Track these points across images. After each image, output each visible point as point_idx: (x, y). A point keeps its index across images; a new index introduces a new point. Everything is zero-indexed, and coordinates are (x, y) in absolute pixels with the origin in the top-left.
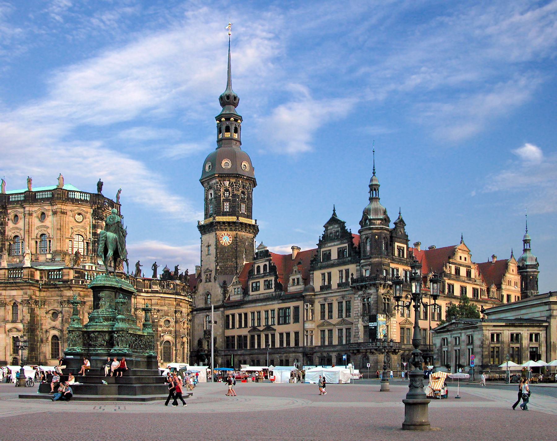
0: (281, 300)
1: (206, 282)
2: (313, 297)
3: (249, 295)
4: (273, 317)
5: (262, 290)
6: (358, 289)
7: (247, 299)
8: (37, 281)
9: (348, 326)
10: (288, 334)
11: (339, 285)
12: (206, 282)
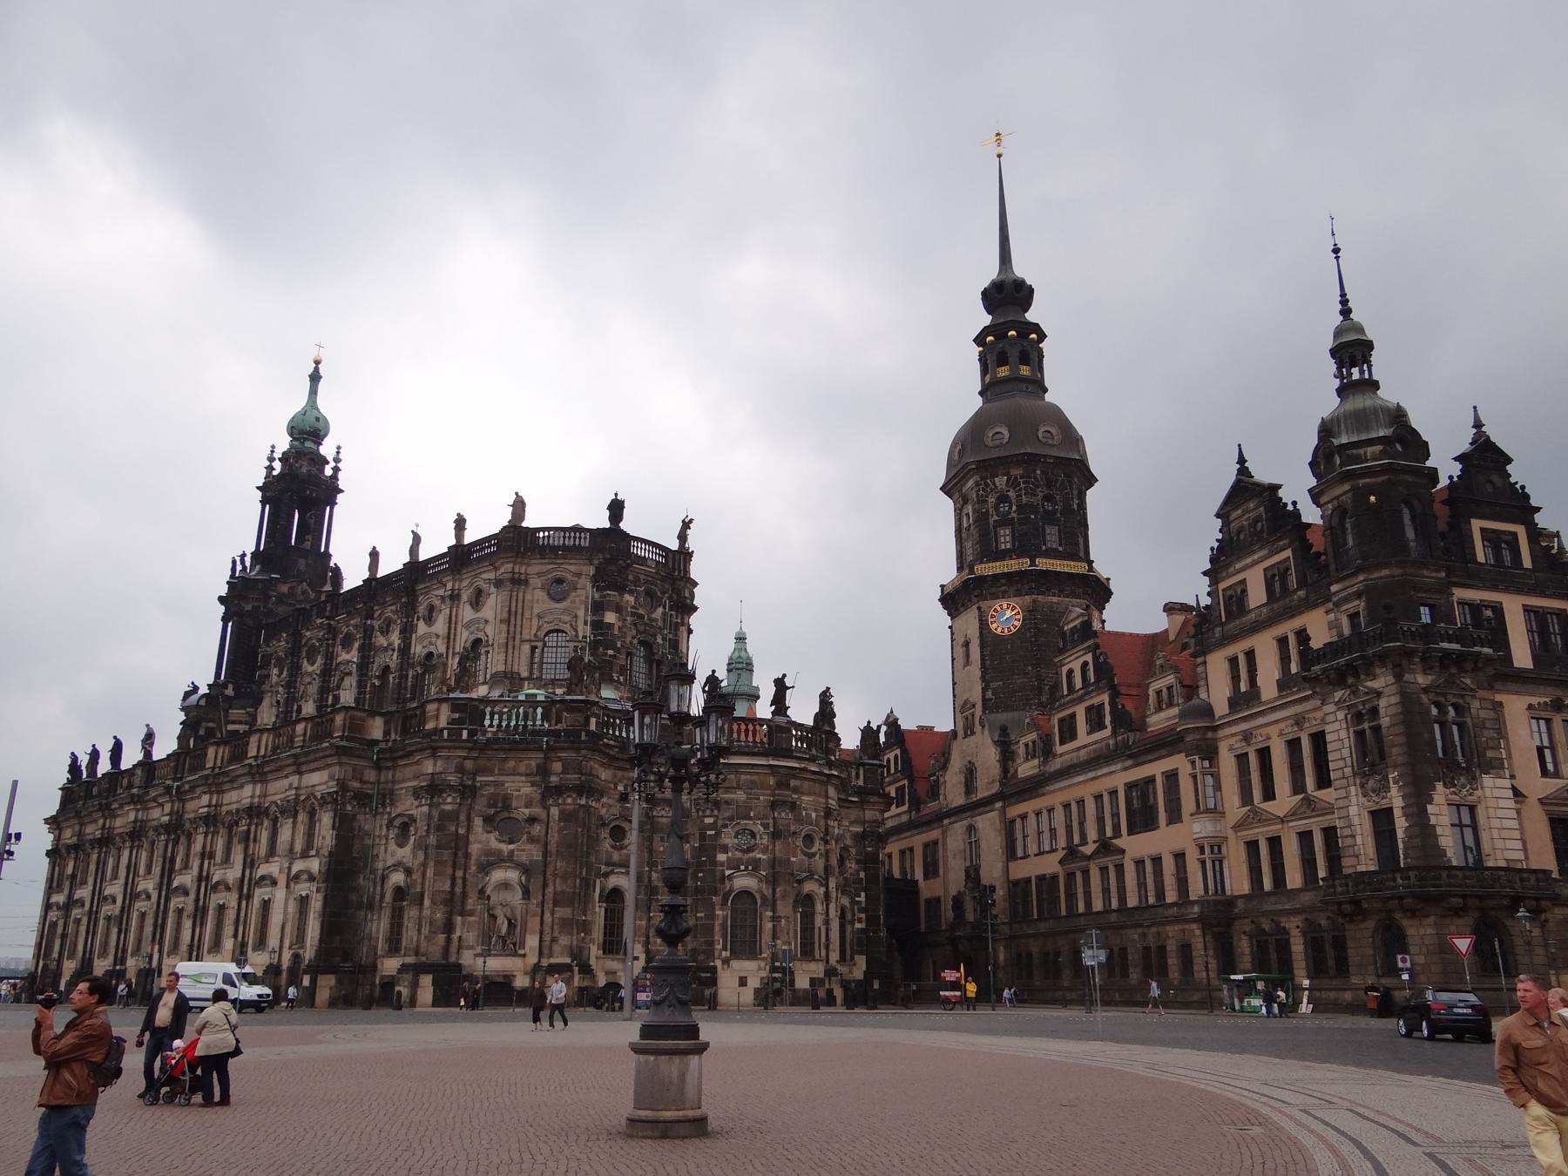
0: (1130, 756)
1: (966, 736)
2: (1210, 735)
3: (1055, 756)
4: (1116, 815)
5: (1083, 737)
6: (1330, 683)
7: (1057, 764)
8: (375, 742)
9: (1326, 821)
10: (1157, 860)
11: (1284, 684)
12: (966, 736)
